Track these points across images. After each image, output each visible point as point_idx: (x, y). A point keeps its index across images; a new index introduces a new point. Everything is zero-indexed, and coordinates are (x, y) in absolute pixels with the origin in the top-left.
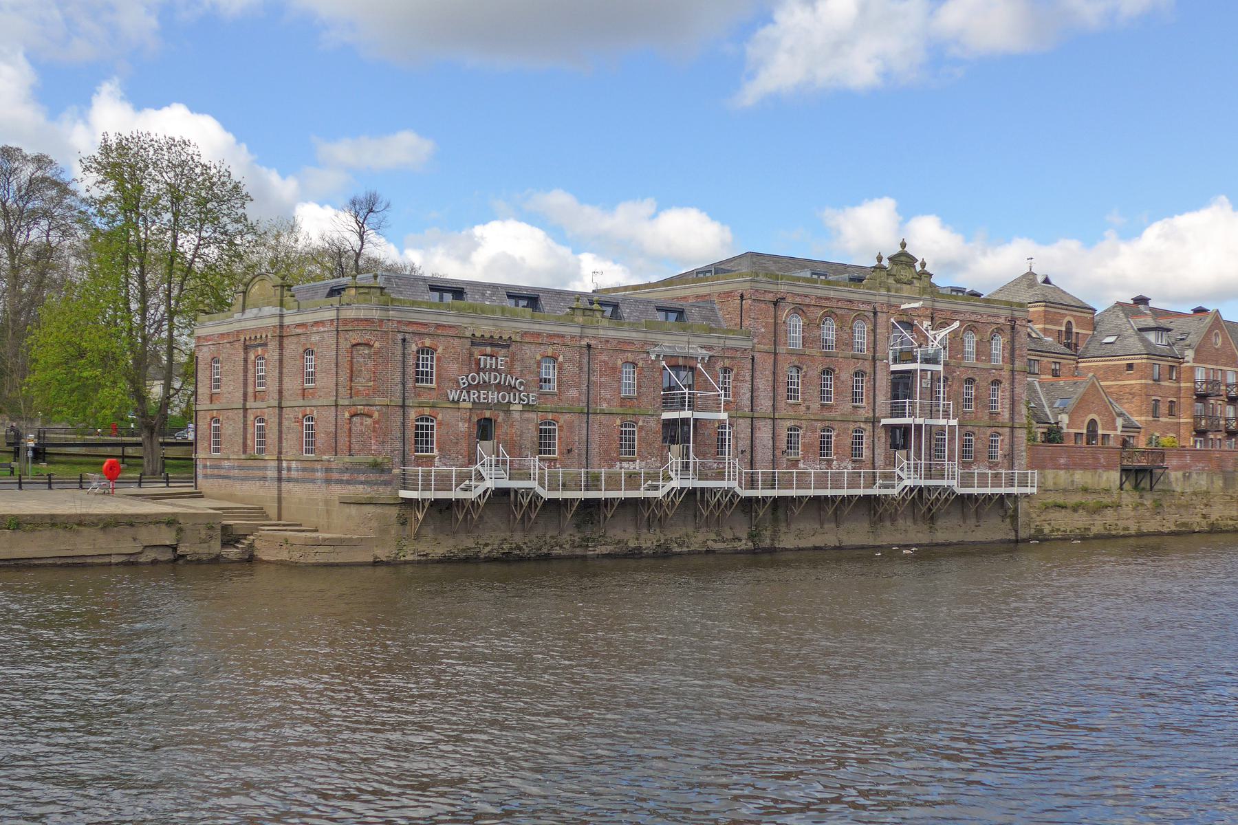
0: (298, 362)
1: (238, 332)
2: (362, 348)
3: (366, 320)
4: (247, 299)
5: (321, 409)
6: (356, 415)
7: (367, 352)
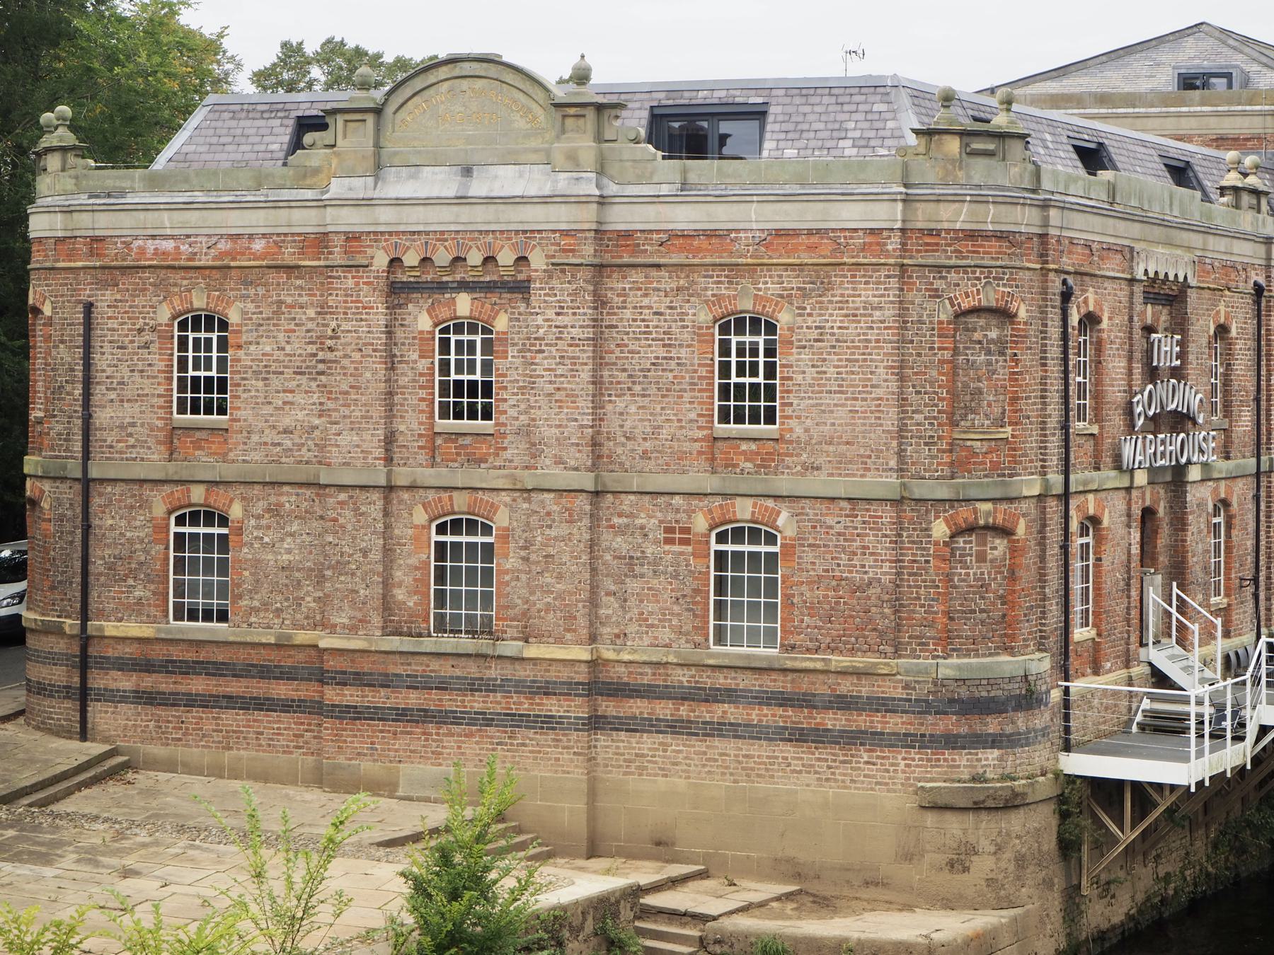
0: (684, 353)
1: (352, 238)
2: (982, 322)
3: (1000, 236)
4: (387, 132)
5: (810, 510)
6: (971, 529)
7: (993, 334)
